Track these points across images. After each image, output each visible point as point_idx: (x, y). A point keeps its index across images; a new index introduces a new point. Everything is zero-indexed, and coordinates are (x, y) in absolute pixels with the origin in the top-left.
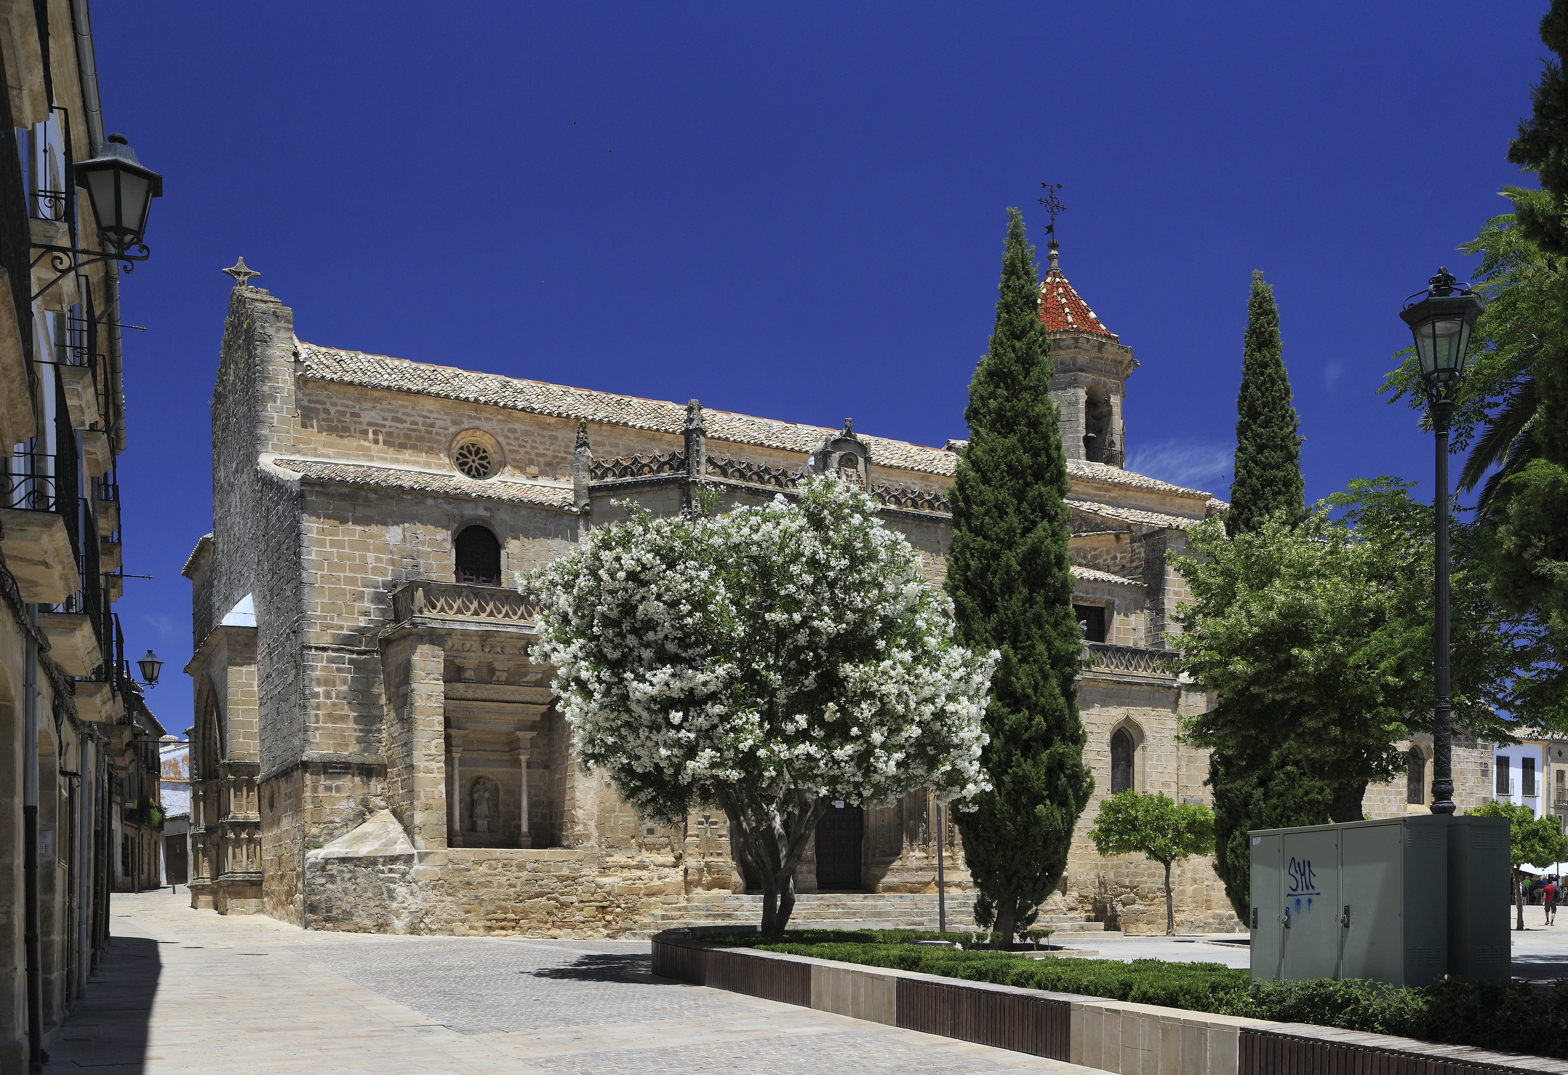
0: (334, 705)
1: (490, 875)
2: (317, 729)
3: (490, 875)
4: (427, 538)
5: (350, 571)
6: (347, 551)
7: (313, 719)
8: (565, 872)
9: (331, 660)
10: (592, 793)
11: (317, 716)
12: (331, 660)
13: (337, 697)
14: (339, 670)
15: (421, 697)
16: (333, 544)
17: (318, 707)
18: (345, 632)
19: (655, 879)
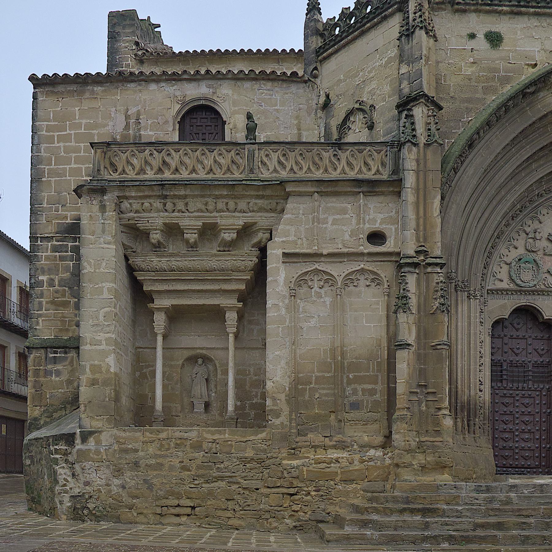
0: (57, 292)
1: (161, 456)
2: (40, 316)
3: (161, 456)
4: (150, 122)
5: (75, 163)
6: (73, 144)
7: (36, 306)
8: (250, 453)
9: (55, 249)
10: (283, 362)
11: (40, 303)
12: (55, 249)
13: (60, 285)
14: (62, 258)
15: (89, 263)
16: (61, 139)
17: (42, 295)
18: (69, 221)
19: (356, 462)
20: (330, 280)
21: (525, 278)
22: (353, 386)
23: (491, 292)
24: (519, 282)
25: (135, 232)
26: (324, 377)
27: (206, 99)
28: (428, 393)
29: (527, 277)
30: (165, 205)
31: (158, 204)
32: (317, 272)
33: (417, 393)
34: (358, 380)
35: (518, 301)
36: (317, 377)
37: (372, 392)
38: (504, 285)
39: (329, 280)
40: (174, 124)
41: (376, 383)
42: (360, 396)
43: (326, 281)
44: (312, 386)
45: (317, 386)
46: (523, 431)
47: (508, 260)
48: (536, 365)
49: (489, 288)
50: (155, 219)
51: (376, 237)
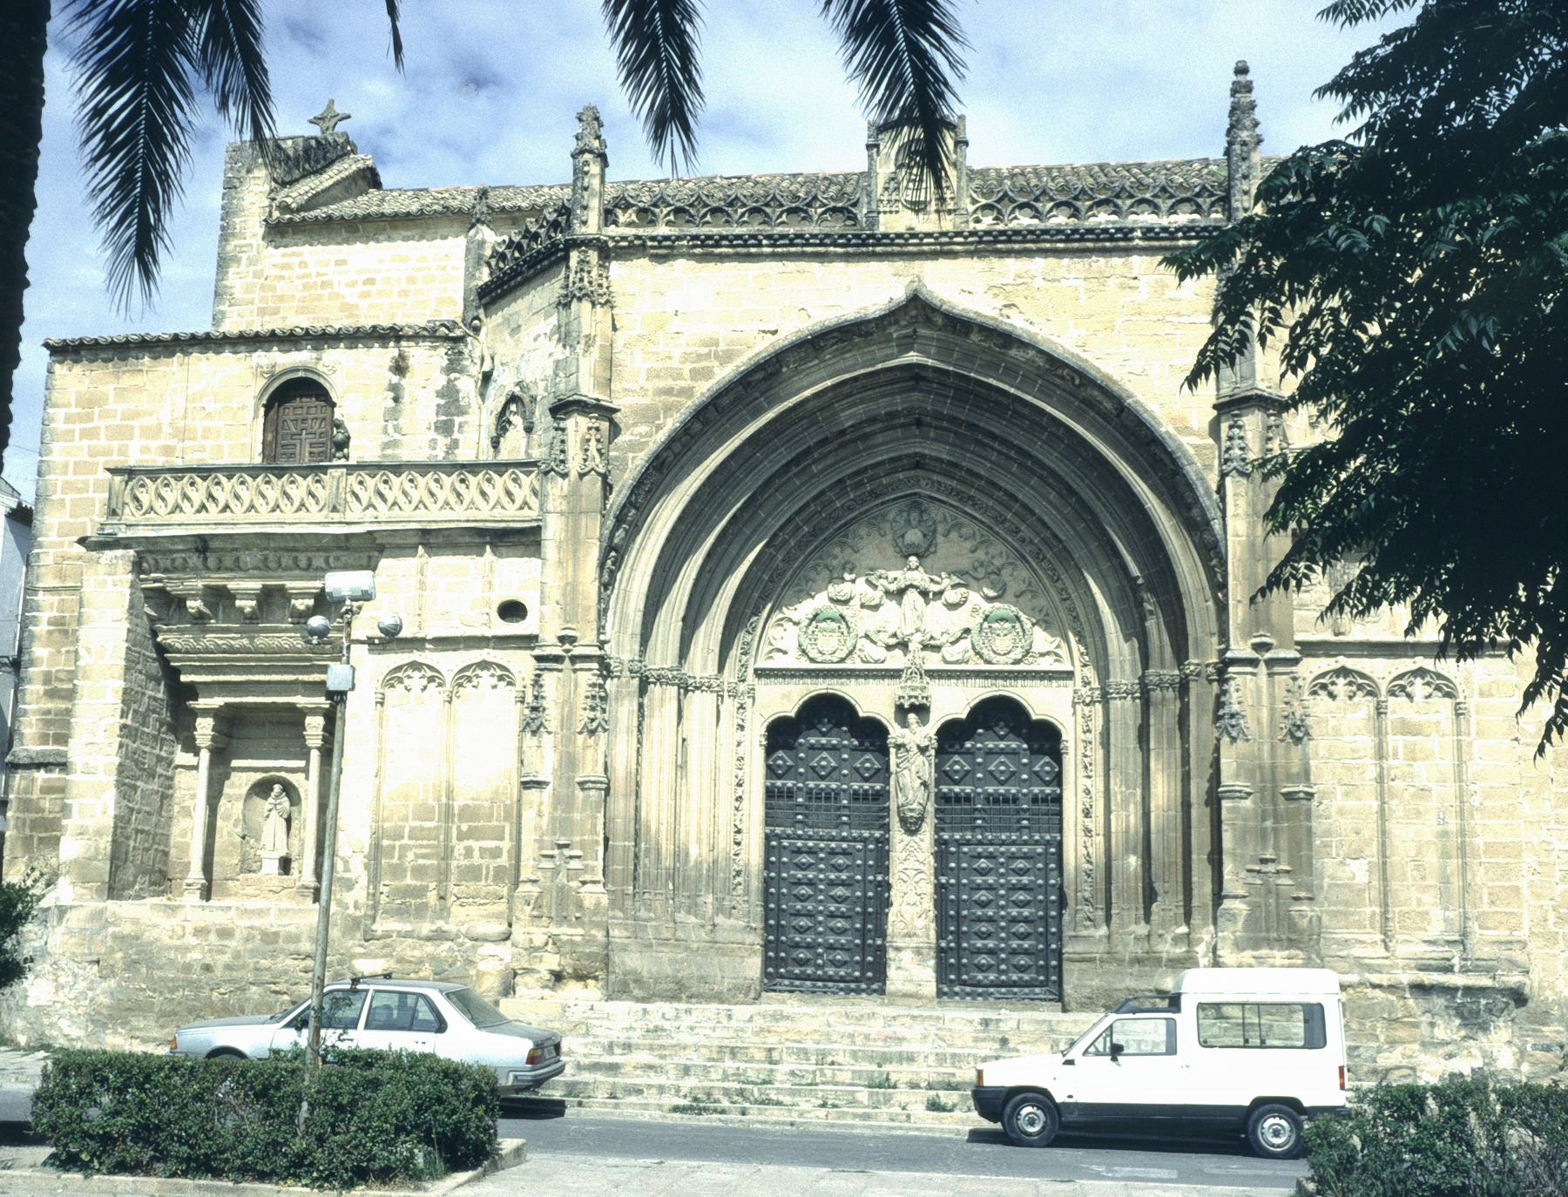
20: (435, 678)
21: (827, 648)
22: (466, 843)
23: (761, 673)
24: (813, 654)
25: (167, 604)
26: (422, 829)
27: (306, 370)
28: (571, 857)
29: (829, 646)
30: (206, 559)
31: (195, 560)
32: (416, 666)
33: (552, 857)
34: (472, 834)
35: (812, 688)
36: (412, 829)
37: (495, 854)
38: (779, 662)
39: (435, 678)
40: (256, 411)
41: (502, 839)
42: (476, 859)
43: (431, 679)
44: (403, 842)
45: (412, 842)
46: (832, 916)
47: (796, 619)
48: (856, 796)
49: (760, 665)
50: (192, 585)
51: (512, 610)
